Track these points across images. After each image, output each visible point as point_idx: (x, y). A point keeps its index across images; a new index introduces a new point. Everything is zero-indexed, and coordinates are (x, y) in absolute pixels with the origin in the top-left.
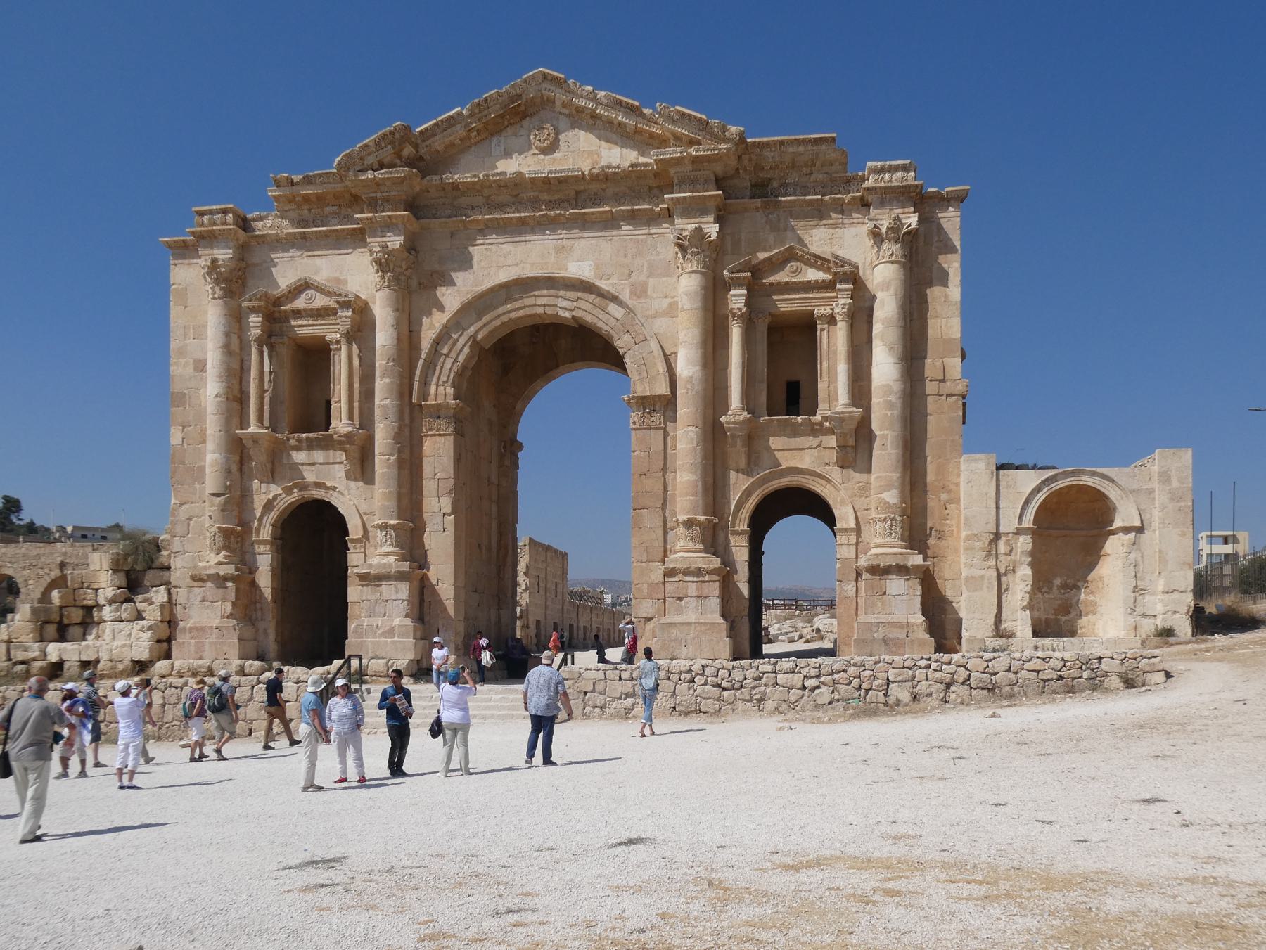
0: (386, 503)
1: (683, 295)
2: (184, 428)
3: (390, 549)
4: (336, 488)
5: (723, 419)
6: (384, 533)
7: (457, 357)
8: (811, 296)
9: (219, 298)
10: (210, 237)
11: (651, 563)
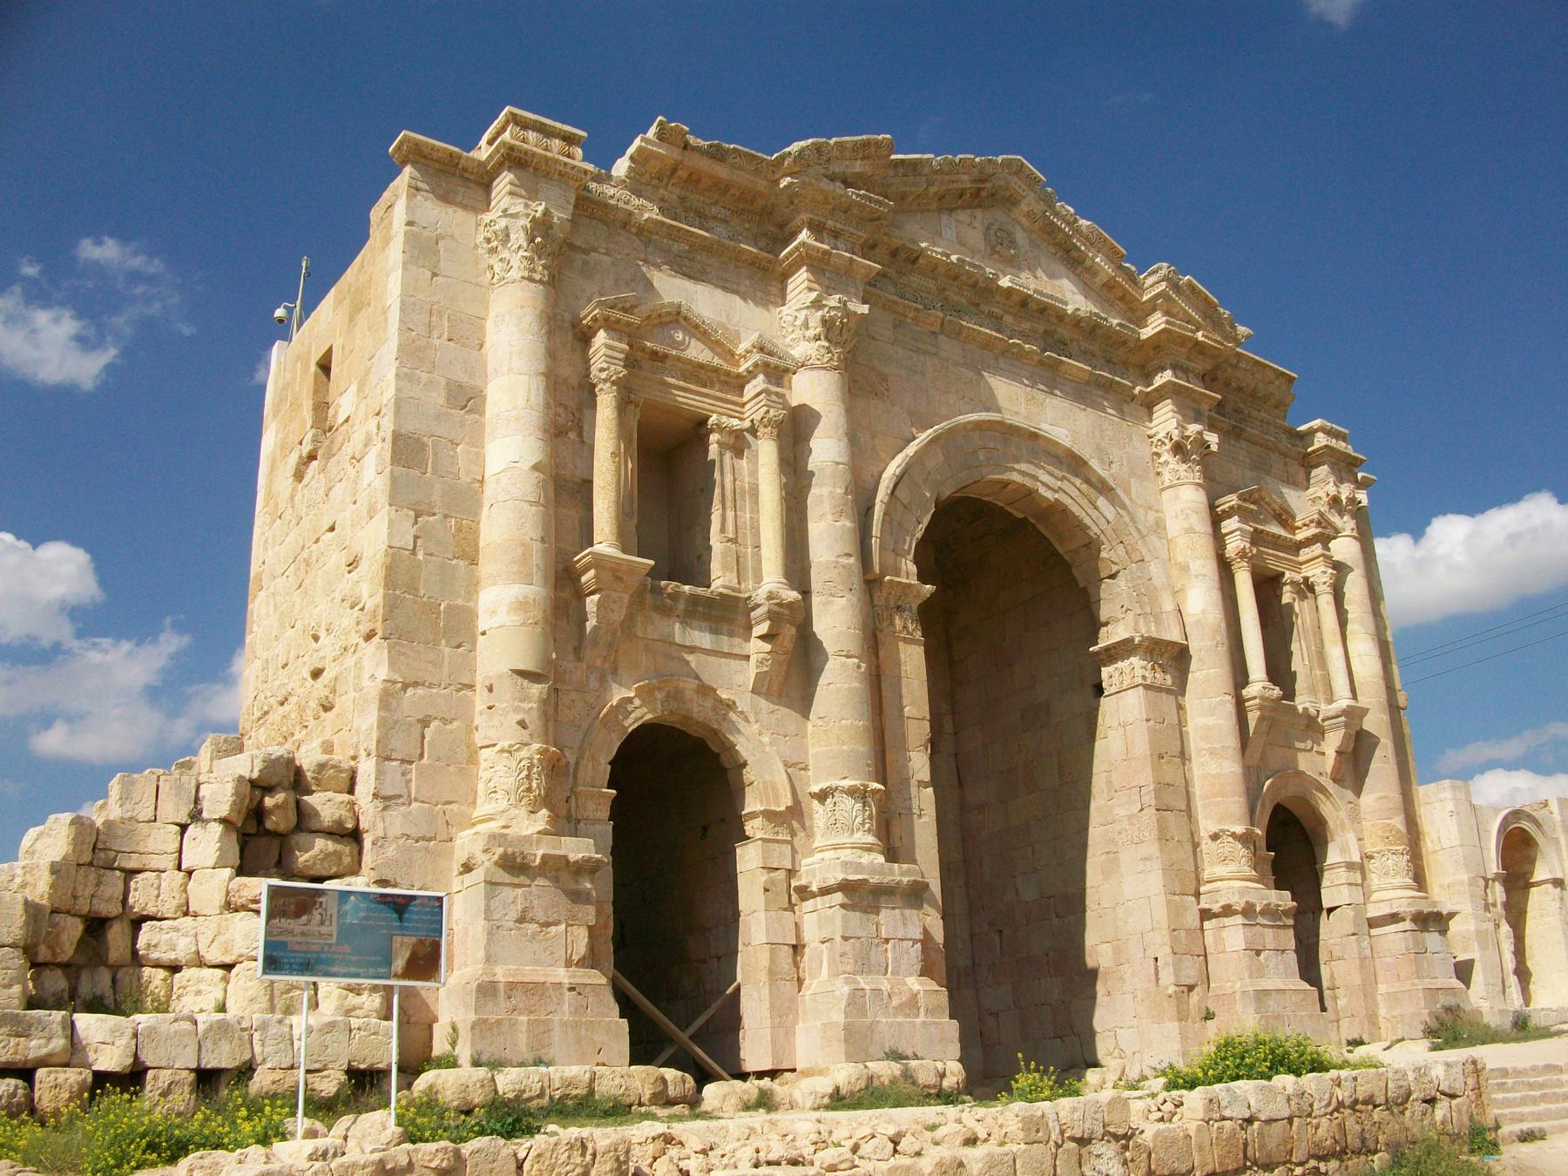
0: (862, 749)
1: (1190, 512)
2: (417, 517)
3: (871, 839)
5: (1246, 692)
8: (1281, 554)
9: (540, 282)
10: (536, 169)
11: (1185, 897)
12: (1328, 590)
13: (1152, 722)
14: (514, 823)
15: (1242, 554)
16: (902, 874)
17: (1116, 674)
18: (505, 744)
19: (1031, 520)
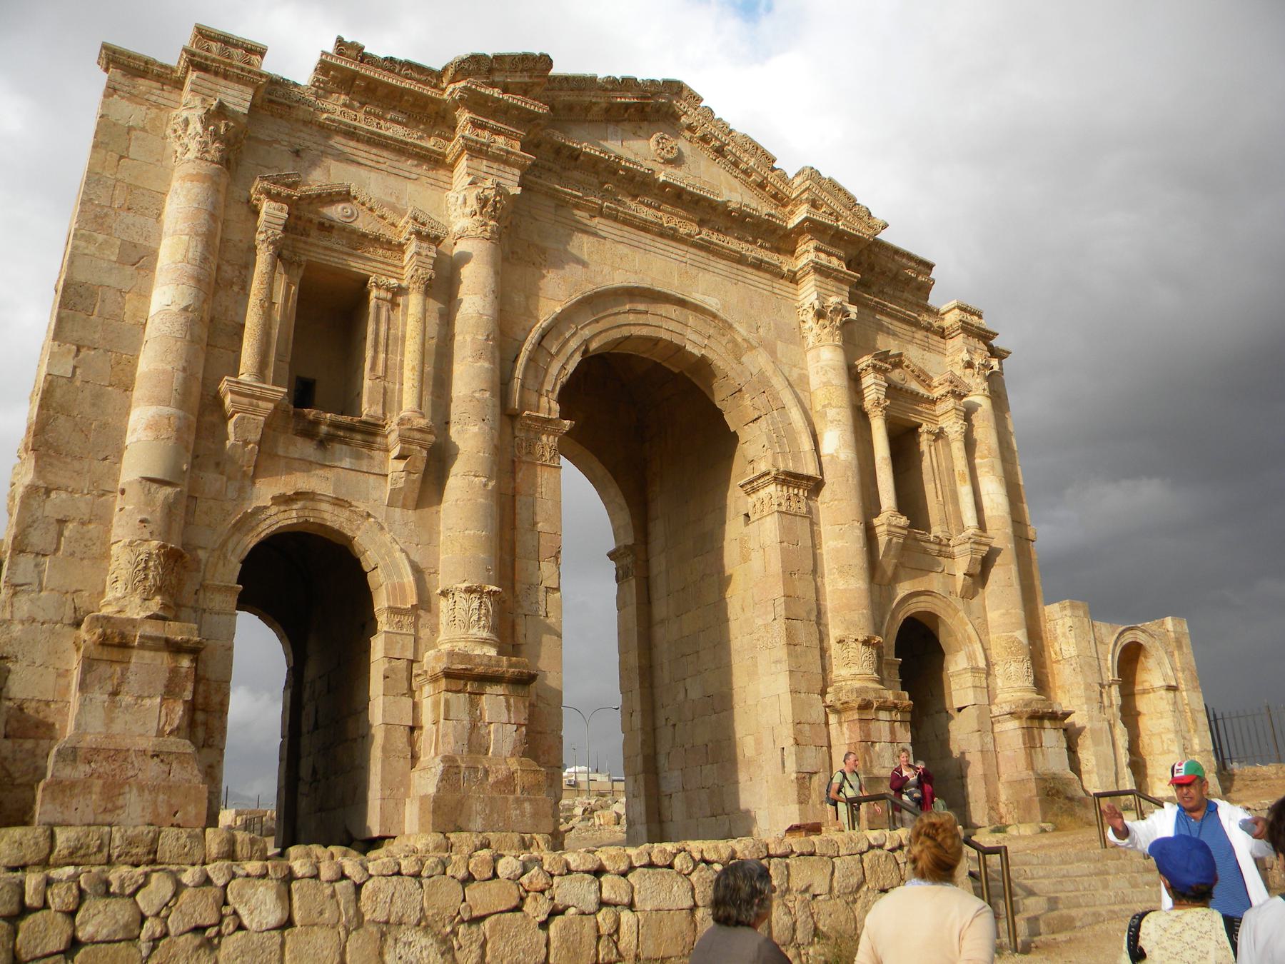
2: (78, 350)
3: (485, 634)
4: (369, 515)
6: (476, 604)
7: (566, 363)
12: (959, 437)
13: (785, 544)
14: (128, 610)
15: (877, 403)
16: (510, 666)
17: (758, 505)
18: (127, 540)
19: (687, 374)
